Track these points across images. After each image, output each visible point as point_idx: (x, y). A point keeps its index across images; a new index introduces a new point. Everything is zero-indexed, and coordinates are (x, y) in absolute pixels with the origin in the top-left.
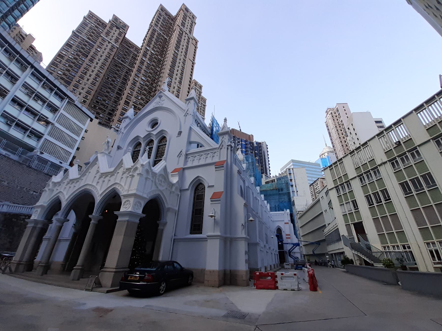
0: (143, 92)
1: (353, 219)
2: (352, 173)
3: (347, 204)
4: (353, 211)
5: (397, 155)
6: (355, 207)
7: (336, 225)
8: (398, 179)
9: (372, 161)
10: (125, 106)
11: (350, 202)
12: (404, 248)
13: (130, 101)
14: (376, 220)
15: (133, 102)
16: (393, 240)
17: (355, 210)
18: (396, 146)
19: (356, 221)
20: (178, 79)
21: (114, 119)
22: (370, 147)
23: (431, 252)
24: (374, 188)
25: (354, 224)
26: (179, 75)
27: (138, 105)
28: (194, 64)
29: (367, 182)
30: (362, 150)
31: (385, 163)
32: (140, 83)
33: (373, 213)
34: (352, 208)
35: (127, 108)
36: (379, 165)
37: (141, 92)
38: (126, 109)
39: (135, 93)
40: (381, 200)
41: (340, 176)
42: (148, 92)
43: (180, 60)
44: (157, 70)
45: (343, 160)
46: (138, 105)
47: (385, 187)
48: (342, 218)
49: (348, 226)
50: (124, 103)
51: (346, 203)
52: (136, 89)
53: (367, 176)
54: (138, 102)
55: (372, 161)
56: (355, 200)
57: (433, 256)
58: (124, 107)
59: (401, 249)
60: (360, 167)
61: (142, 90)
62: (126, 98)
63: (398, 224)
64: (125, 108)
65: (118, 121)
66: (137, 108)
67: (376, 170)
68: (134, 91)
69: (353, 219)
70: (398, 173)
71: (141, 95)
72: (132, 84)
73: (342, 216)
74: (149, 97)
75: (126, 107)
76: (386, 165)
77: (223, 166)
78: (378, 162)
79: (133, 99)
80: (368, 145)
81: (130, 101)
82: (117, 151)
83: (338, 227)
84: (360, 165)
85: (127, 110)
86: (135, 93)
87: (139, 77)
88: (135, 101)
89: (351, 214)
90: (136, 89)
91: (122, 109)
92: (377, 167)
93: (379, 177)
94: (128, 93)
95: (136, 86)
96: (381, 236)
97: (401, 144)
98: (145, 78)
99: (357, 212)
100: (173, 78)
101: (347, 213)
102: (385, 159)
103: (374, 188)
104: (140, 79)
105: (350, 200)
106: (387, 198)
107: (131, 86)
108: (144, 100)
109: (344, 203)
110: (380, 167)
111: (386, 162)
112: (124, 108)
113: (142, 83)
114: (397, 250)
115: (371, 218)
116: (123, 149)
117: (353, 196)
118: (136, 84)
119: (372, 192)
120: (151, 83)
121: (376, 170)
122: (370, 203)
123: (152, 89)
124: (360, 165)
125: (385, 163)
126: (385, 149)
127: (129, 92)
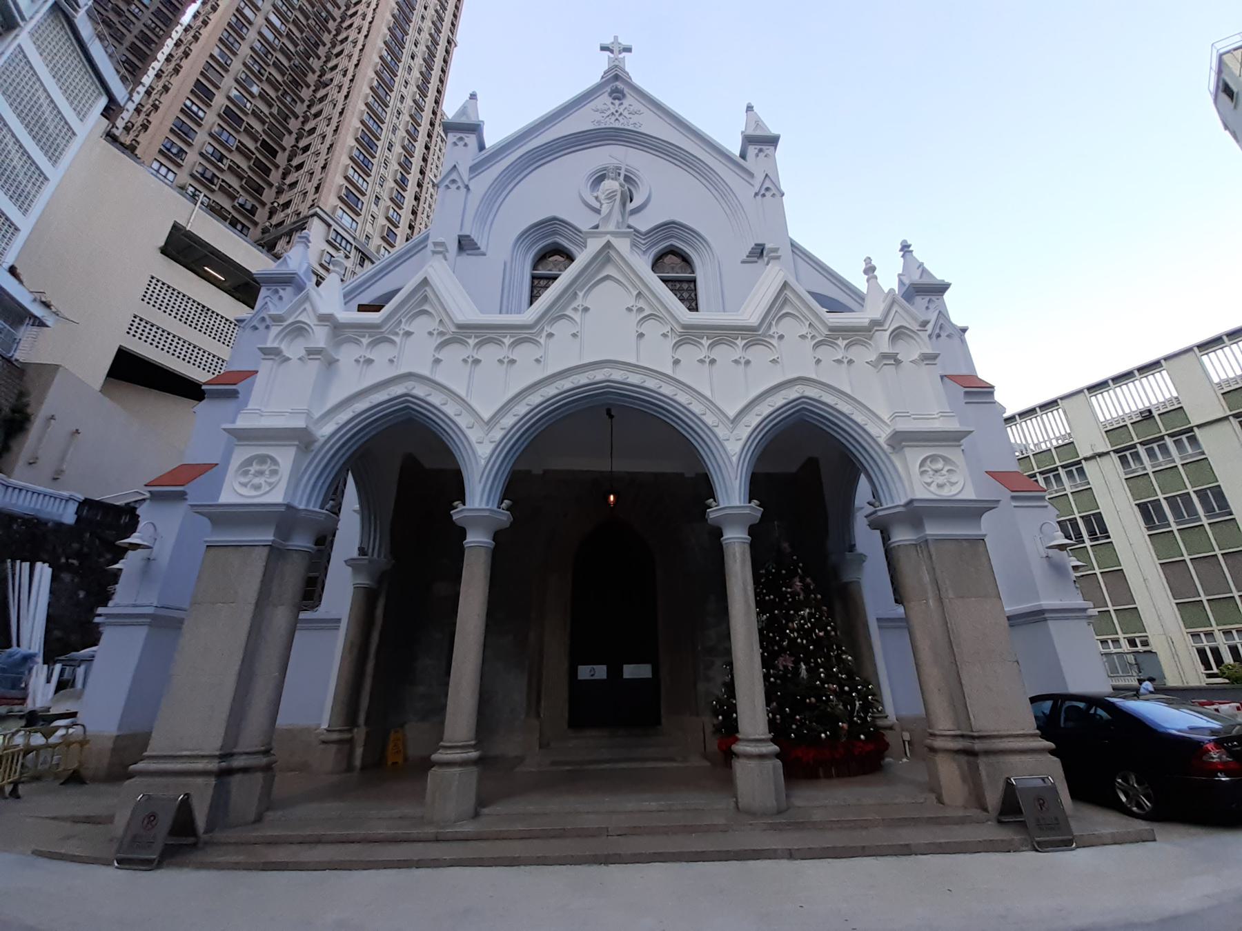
0: (270, 73)
10: (193, 103)
13: (218, 88)
15: (229, 98)
20: (416, 73)
21: (138, 143)
26: (419, 60)
27: (246, 114)
28: (453, 45)
32: (260, 33)
35: (201, 114)
37: (262, 71)
38: (196, 114)
39: (236, 66)
42: (290, 78)
43: (425, 8)
44: (328, 12)
46: (246, 114)
50: (192, 91)
52: (244, 50)
54: (248, 105)
58: (188, 103)
61: (268, 65)
62: (202, 73)
64: (195, 108)
65: (161, 151)
66: (245, 124)
68: (235, 54)
71: (261, 81)
72: (229, 24)
74: (293, 100)
75: (200, 108)
79: (228, 86)
81: (218, 88)
82: (459, 258)
85: (202, 119)
86: (236, 66)
87: (258, 9)
88: (235, 96)
90: (244, 50)
91: (182, 110)
94: (212, 56)
95: (243, 39)
98: (280, 23)
100: (400, 61)
104: (259, 21)
107: (226, 34)
108: (270, 106)
112: (189, 109)
113: (270, 37)
116: (484, 254)
118: (245, 30)
120: (302, 48)
123: (306, 76)
127: (216, 52)
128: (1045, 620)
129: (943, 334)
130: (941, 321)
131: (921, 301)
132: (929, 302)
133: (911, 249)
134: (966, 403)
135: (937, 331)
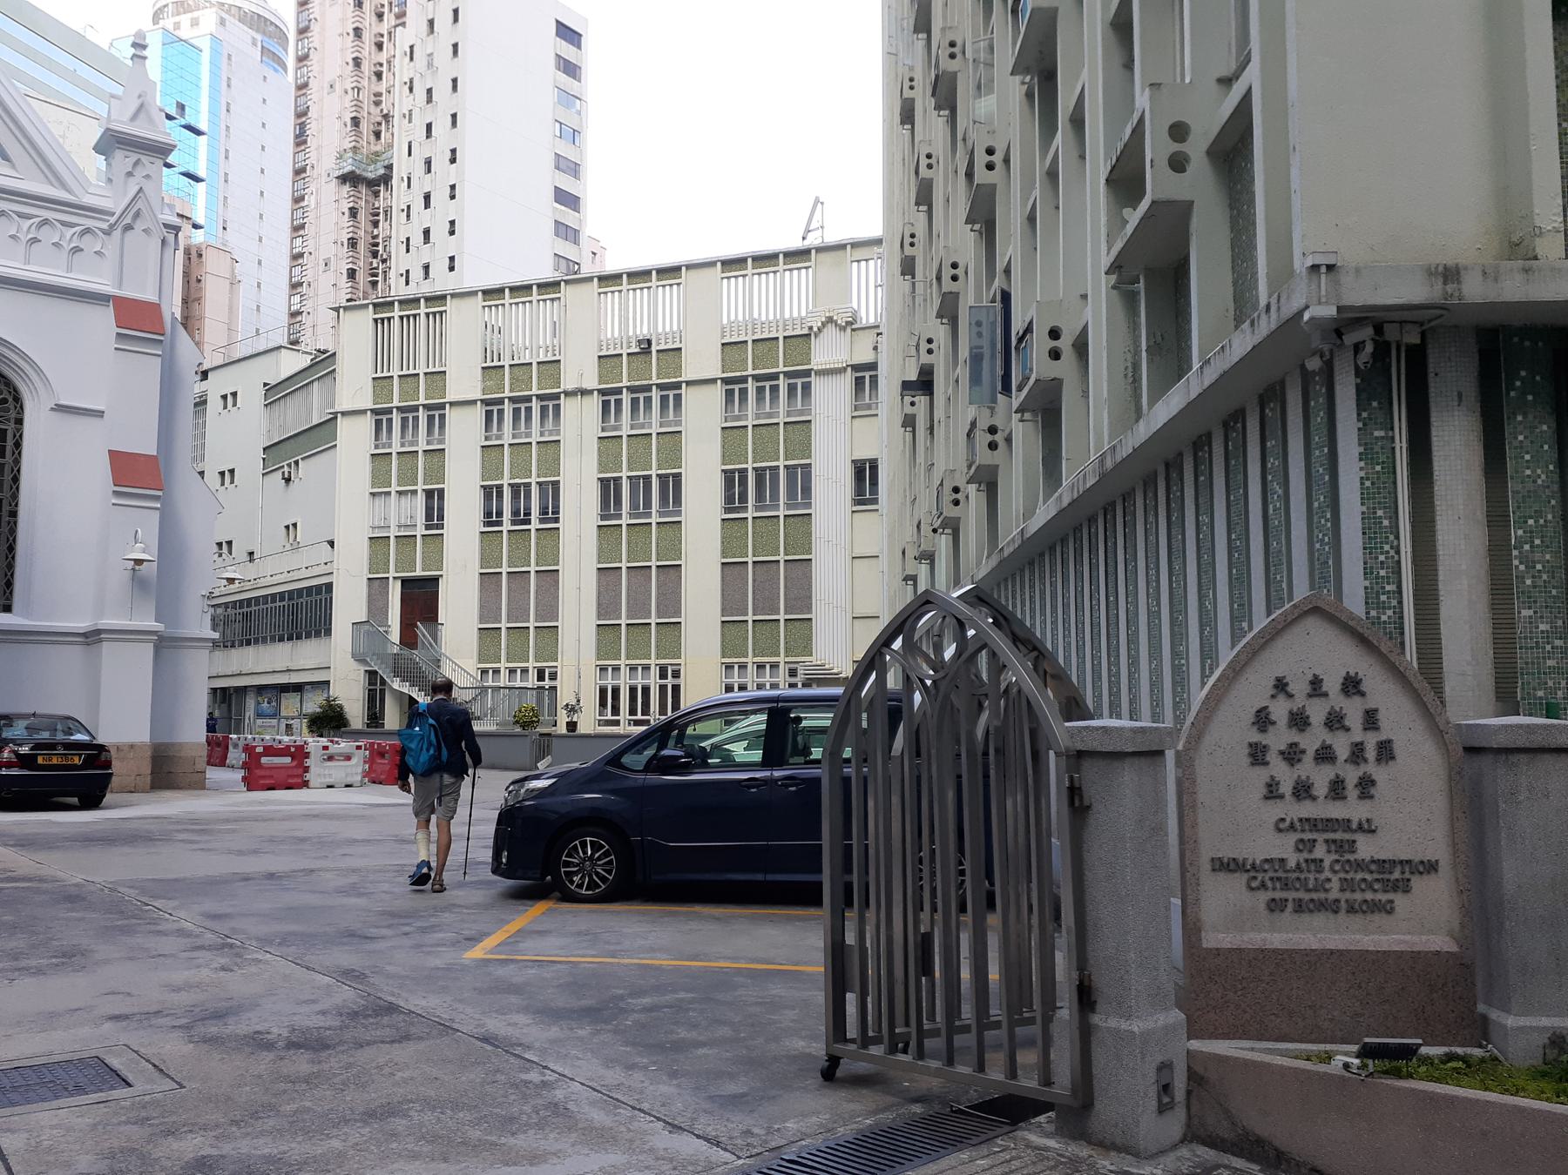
1: (406, 561)
2: (464, 382)
3: (403, 498)
4: (420, 531)
5: (629, 384)
6: (429, 516)
7: (326, 569)
8: (602, 467)
9: (551, 366)
11: (419, 492)
12: (541, 677)
14: (488, 580)
16: (518, 653)
17: (426, 529)
18: (637, 350)
19: (419, 572)
22: (563, 308)
23: (603, 691)
24: (521, 467)
25: (405, 582)
29: (507, 439)
30: (535, 302)
31: (584, 392)
33: (489, 554)
34: (420, 518)
36: (567, 394)
40: (530, 514)
41: (412, 371)
45: (450, 305)
47: (559, 475)
48: (363, 550)
49: (377, 586)
51: (400, 493)
53: (516, 412)
55: (551, 366)
56: (443, 490)
57: (603, 704)
59: (532, 681)
60: (503, 366)
63: (549, 608)
67: (551, 403)
69: (406, 561)
70: (608, 442)
73: (366, 543)
76: (587, 399)
77: (161, 341)
78: (568, 383)
80: (559, 298)
83: (333, 579)
84: (506, 362)
89: (406, 540)
92: (556, 397)
93: (550, 435)
96: (488, 634)
97: (651, 352)
99: (435, 540)
101: (393, 532)
102: (592, 382)
103: (521, 467)
105: (420, 487)
106: (551, 513)
109: (394, 488)
110: (568, 399)
111: (590, 392)
114: (518, 684)
115: (475, 569)
117: (436, 472)
119: (512, 481)
121: (551, 404)
122: (491, 518)
124: (506, 362)
125: (584, 392)
126: (604, 347)
128: (101, 641)
129: (139, 226)
130: (139, 205)
131: (125, 161)
132: (137, 163)
133: (145, 53)
134: (116, 349)
135: (128, 220)
